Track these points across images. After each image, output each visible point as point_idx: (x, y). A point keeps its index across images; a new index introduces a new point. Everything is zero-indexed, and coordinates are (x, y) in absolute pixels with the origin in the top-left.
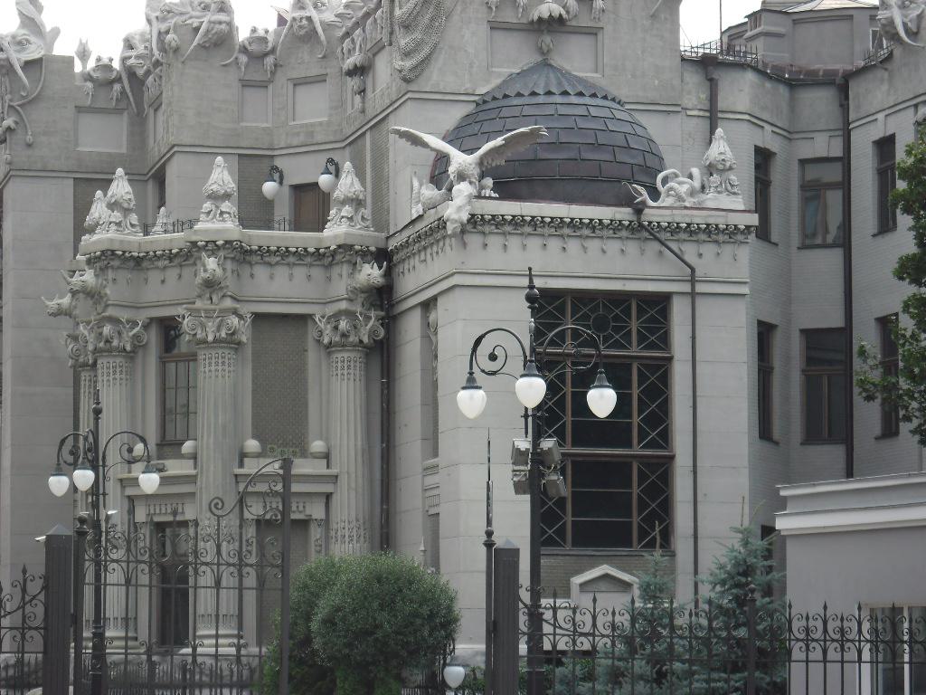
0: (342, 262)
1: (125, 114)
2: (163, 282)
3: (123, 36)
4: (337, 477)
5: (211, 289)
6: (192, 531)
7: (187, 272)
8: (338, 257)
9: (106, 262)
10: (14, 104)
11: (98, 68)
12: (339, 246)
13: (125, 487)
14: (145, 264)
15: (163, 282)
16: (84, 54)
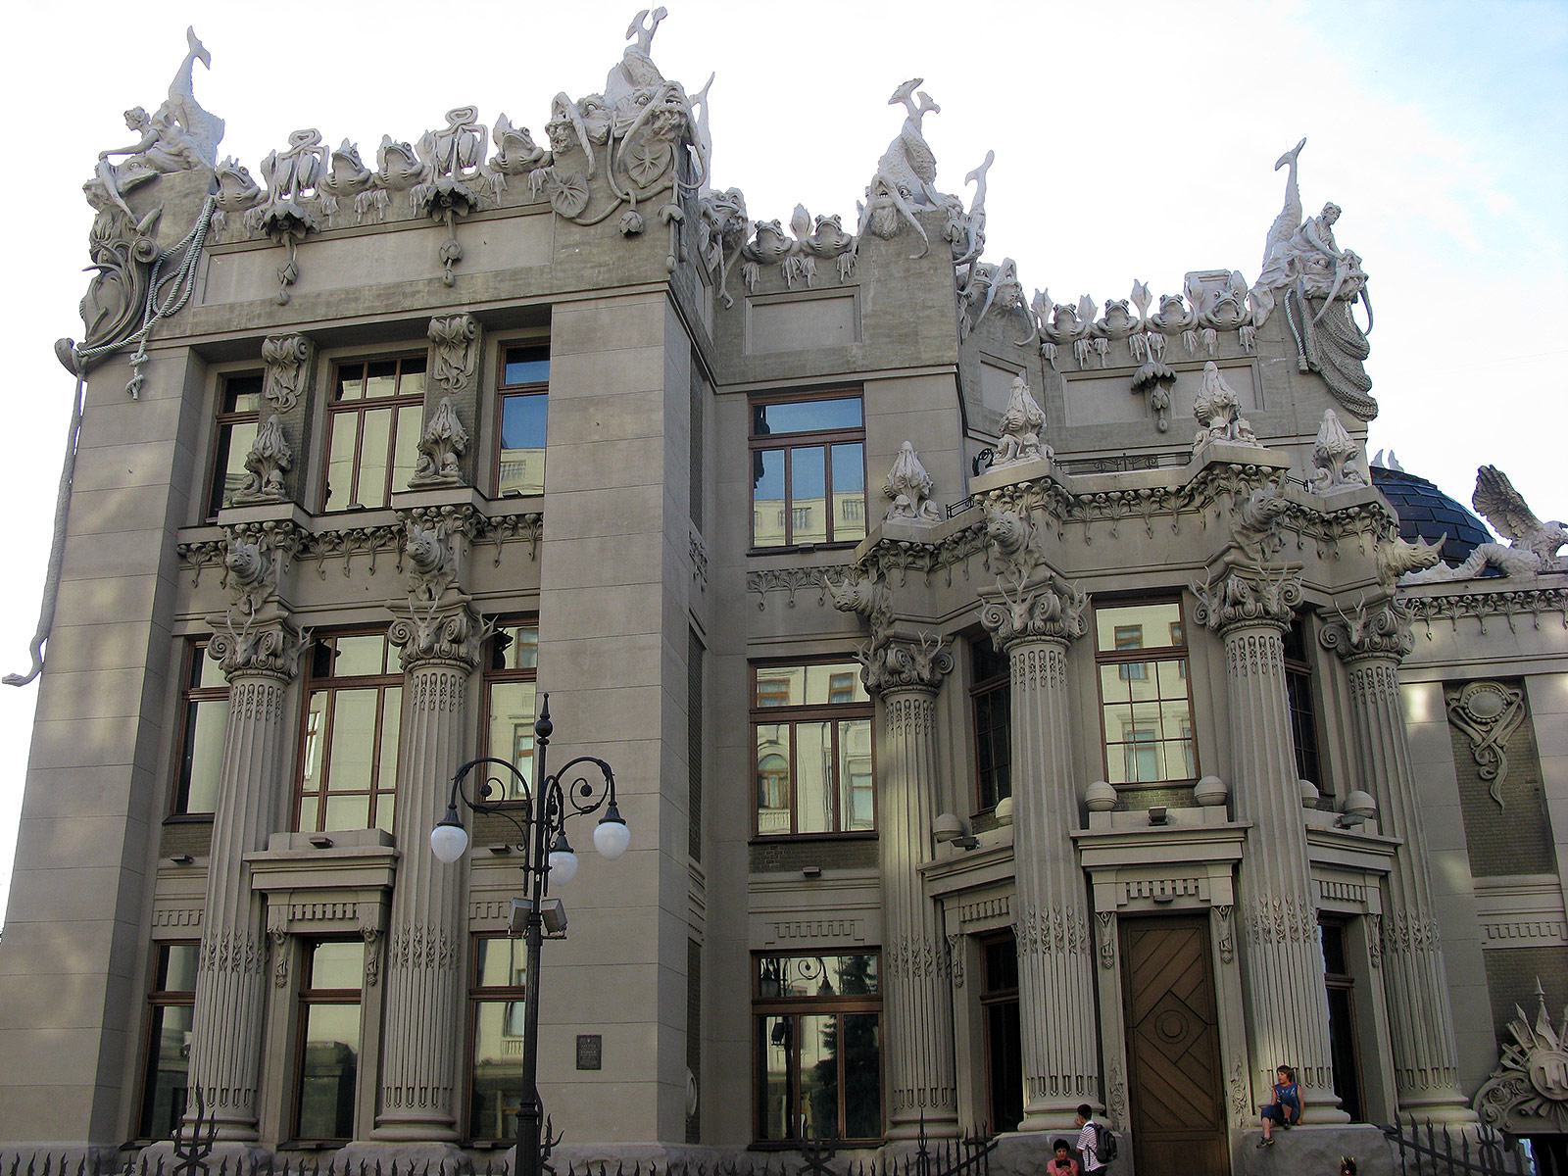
6: (1370, 933)
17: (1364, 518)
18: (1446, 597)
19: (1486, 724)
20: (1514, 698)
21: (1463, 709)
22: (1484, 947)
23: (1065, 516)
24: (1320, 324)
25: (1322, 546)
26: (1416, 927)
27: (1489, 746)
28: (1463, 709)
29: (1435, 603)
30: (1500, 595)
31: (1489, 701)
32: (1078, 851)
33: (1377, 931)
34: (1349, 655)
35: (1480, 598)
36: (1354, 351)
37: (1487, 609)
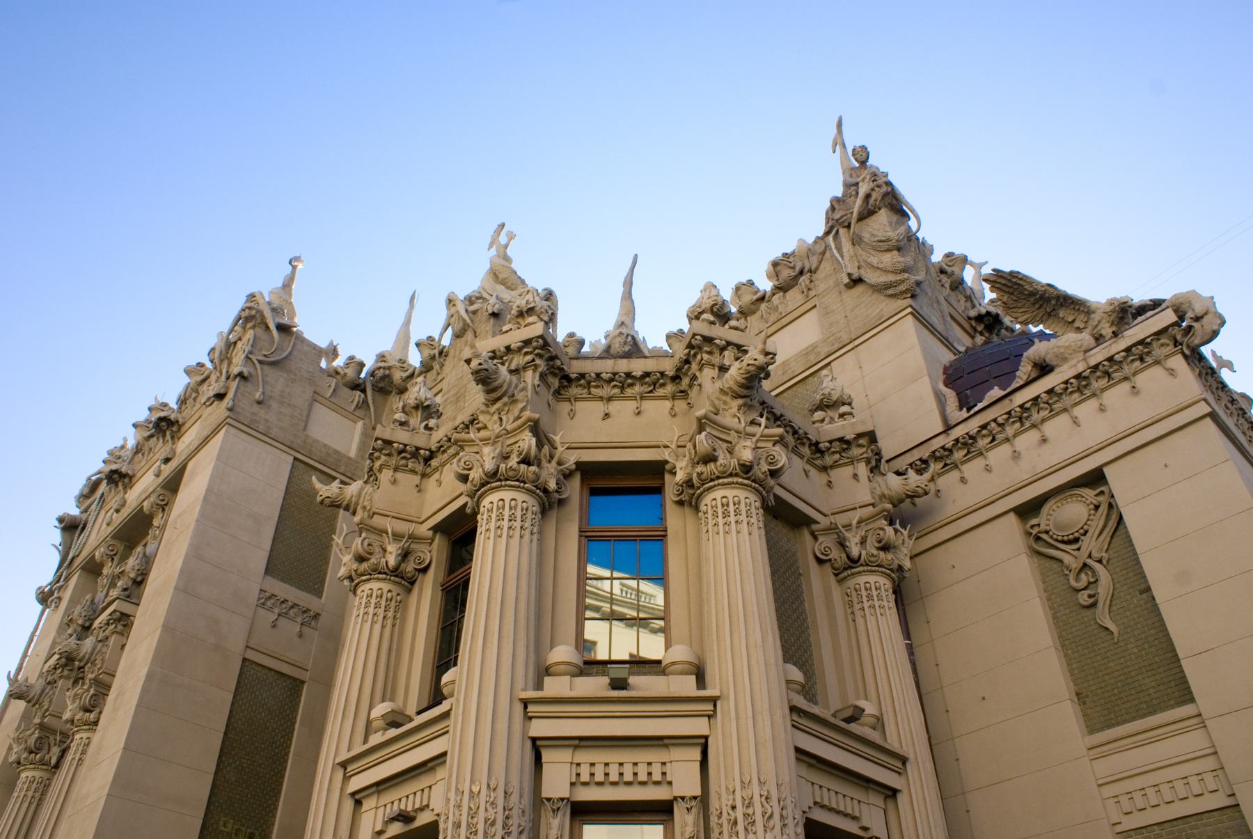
0: (859, 460)
1: (360, 424)
2: (607, 415)
3: (378, 351)
4: (904, 760)
5: (740, 401)
7: (657, 409)
8: (856, 451)
9: (529, 358)
10: (253, 358)
11: (347, 365)
12: (859, 436)
13: (531, 718)
14: (574, 391)
15: (607, 415)
16: (333, 352)
17: (695, 355)
18: (995, 420)
19: (1076, 540)
20: (1101, 498)
21: (1047, 532)
22: (1119, 829)
23: (420, 467)
24: (856, 241)
25: (681, 405)
26: (730, 803)
27: (1085, 565)
28: (1047, 532)
29: (984, 432)
30: (1050, 392)
31: (1072, 513)
32: (346, 778)
33: (690, 818)
34: (691, 498)
35: (1027, 405)
36: (885, 246)
37: (1044, 413)
